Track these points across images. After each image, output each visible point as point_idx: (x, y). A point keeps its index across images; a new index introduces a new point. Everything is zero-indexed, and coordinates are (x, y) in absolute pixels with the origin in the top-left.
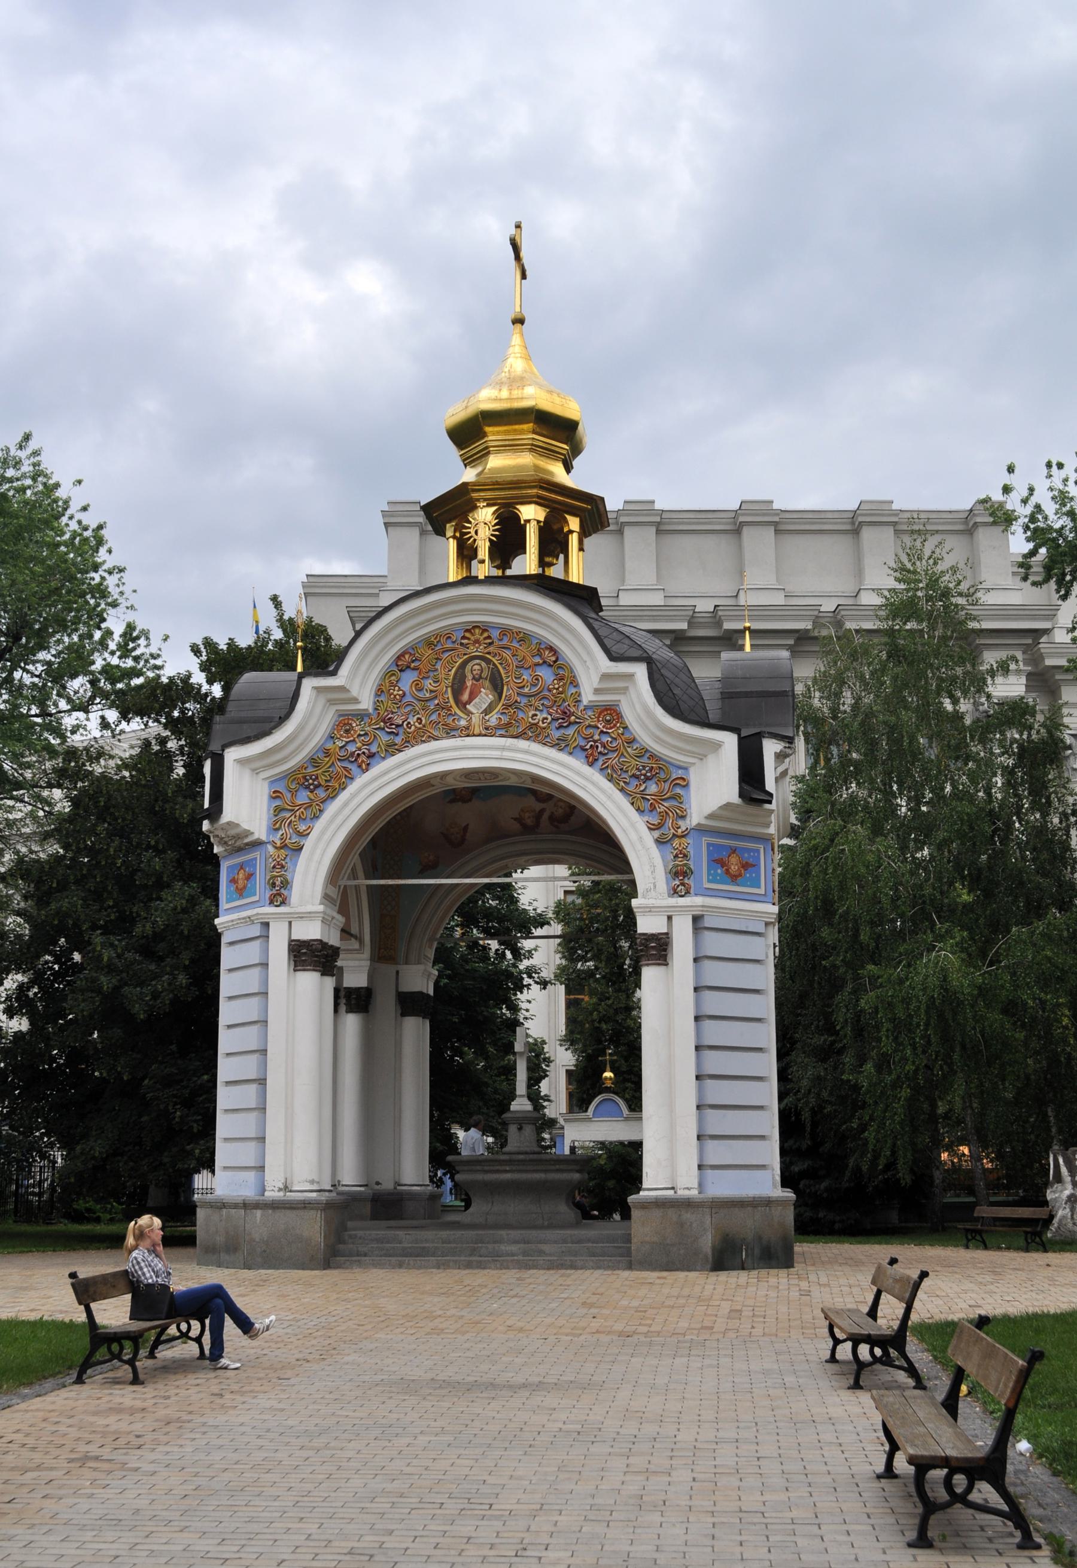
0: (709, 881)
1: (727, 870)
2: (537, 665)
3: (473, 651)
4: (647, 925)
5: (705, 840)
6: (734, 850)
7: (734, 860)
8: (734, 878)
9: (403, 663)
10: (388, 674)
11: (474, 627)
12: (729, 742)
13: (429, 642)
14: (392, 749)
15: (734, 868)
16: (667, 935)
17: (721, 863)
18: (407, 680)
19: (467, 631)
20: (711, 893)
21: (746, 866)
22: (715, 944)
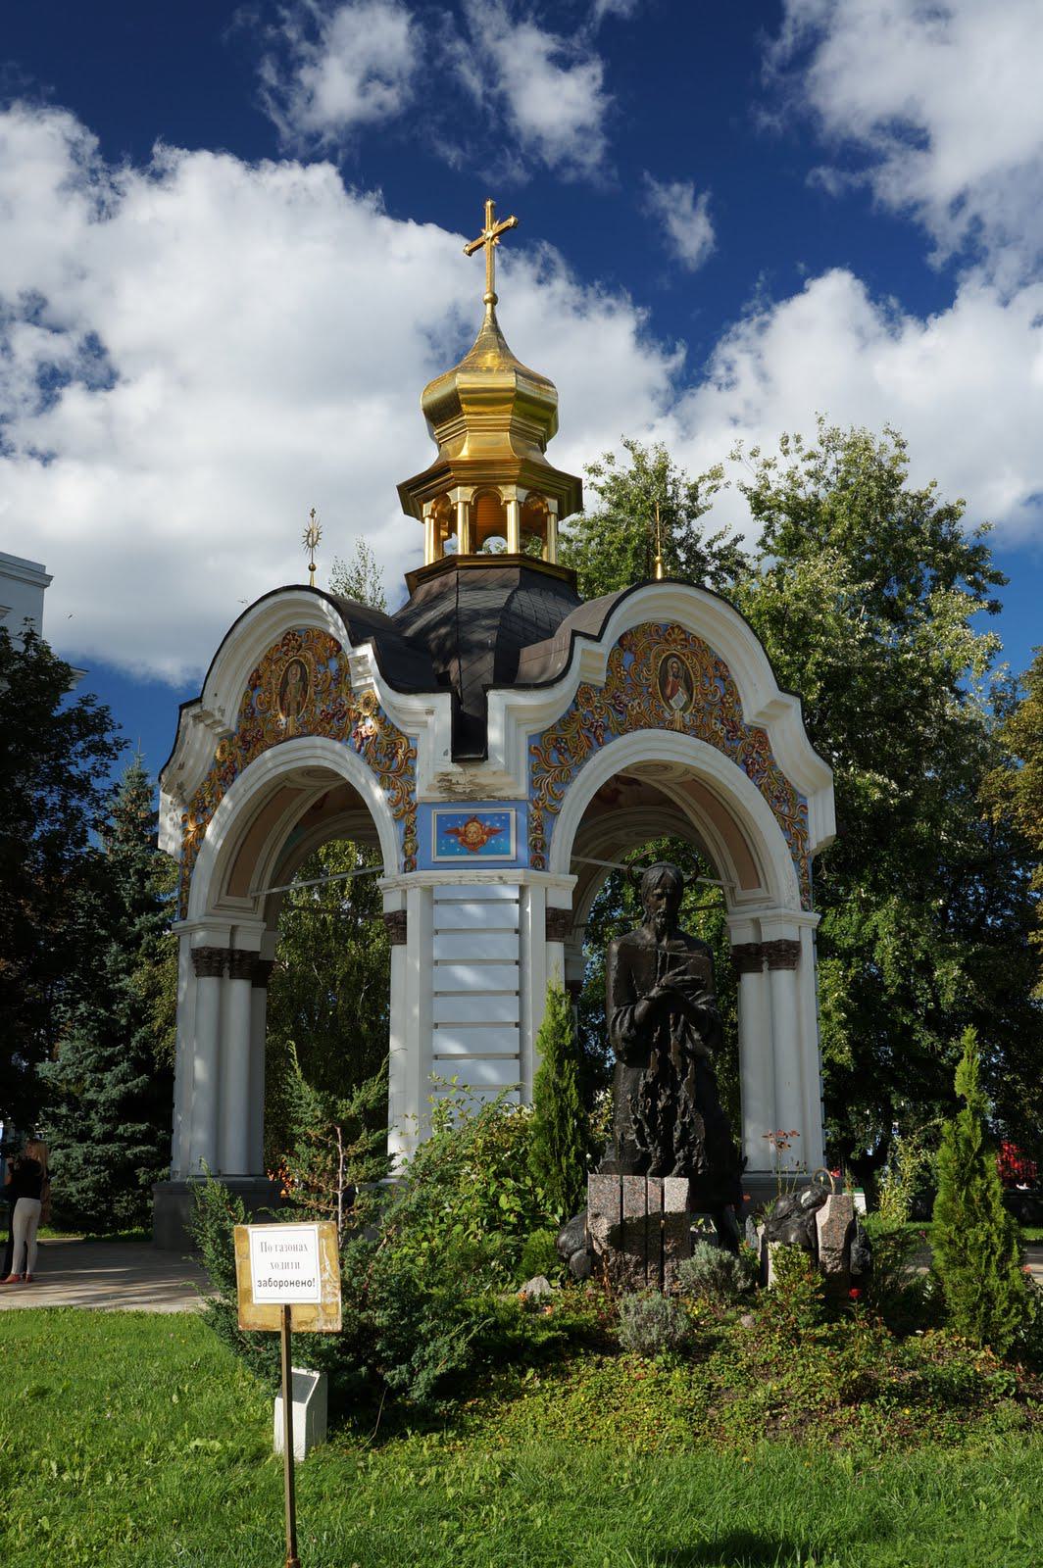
0: (440, 853)
1: (464, 841)
2: (328, 659)
3: (292, 656)
4: (390, 904)
5: (435, 812)
6: (474, 819)
7: (473, 828)
8: (473, 847)
9: (255, 681)
10: (246, 694)
11: (289, 633)
12: (443, 702)
13: (267, 658)
14: (247, 762)
15: (472, 837)
16: (405, 912)
17: (457, 833)
18: (256, 694)
19: (284, 638)
20: (480, 865)
21: (492, 832)
22: (445, 916)
